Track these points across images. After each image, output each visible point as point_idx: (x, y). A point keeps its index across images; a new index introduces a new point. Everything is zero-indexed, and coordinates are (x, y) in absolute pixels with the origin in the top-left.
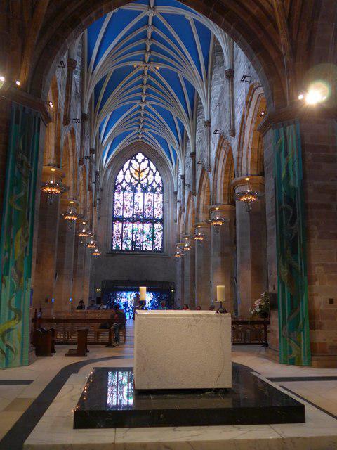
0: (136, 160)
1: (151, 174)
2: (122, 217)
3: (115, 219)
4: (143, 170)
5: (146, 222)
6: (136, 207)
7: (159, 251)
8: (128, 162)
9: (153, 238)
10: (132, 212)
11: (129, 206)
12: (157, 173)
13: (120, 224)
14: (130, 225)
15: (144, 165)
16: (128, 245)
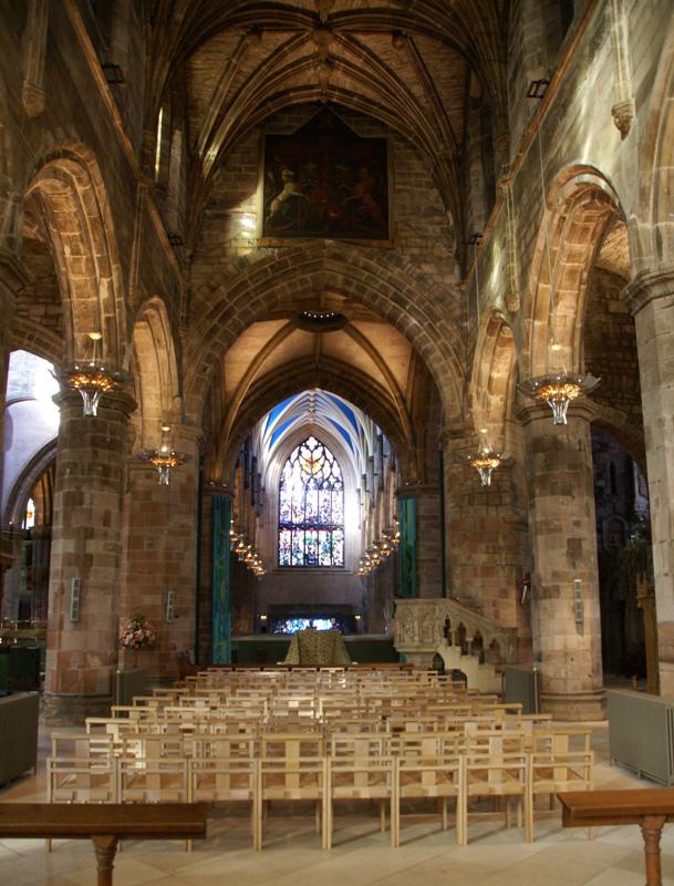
0: (307, 447)
1: (327, 464)
2: (291, 523)
3: (282, 526)
4: (317, 461)
5: (322, 529)
6: (308, 509)
7: (339, 567)
8: (297, 450)
9: (332, 549)
10: (302, 516)
11: (299, 509)
12: (335, 464)
13: (289, 532)
14: (300, 534)
15: (317, 454)
16: (299, 560)
